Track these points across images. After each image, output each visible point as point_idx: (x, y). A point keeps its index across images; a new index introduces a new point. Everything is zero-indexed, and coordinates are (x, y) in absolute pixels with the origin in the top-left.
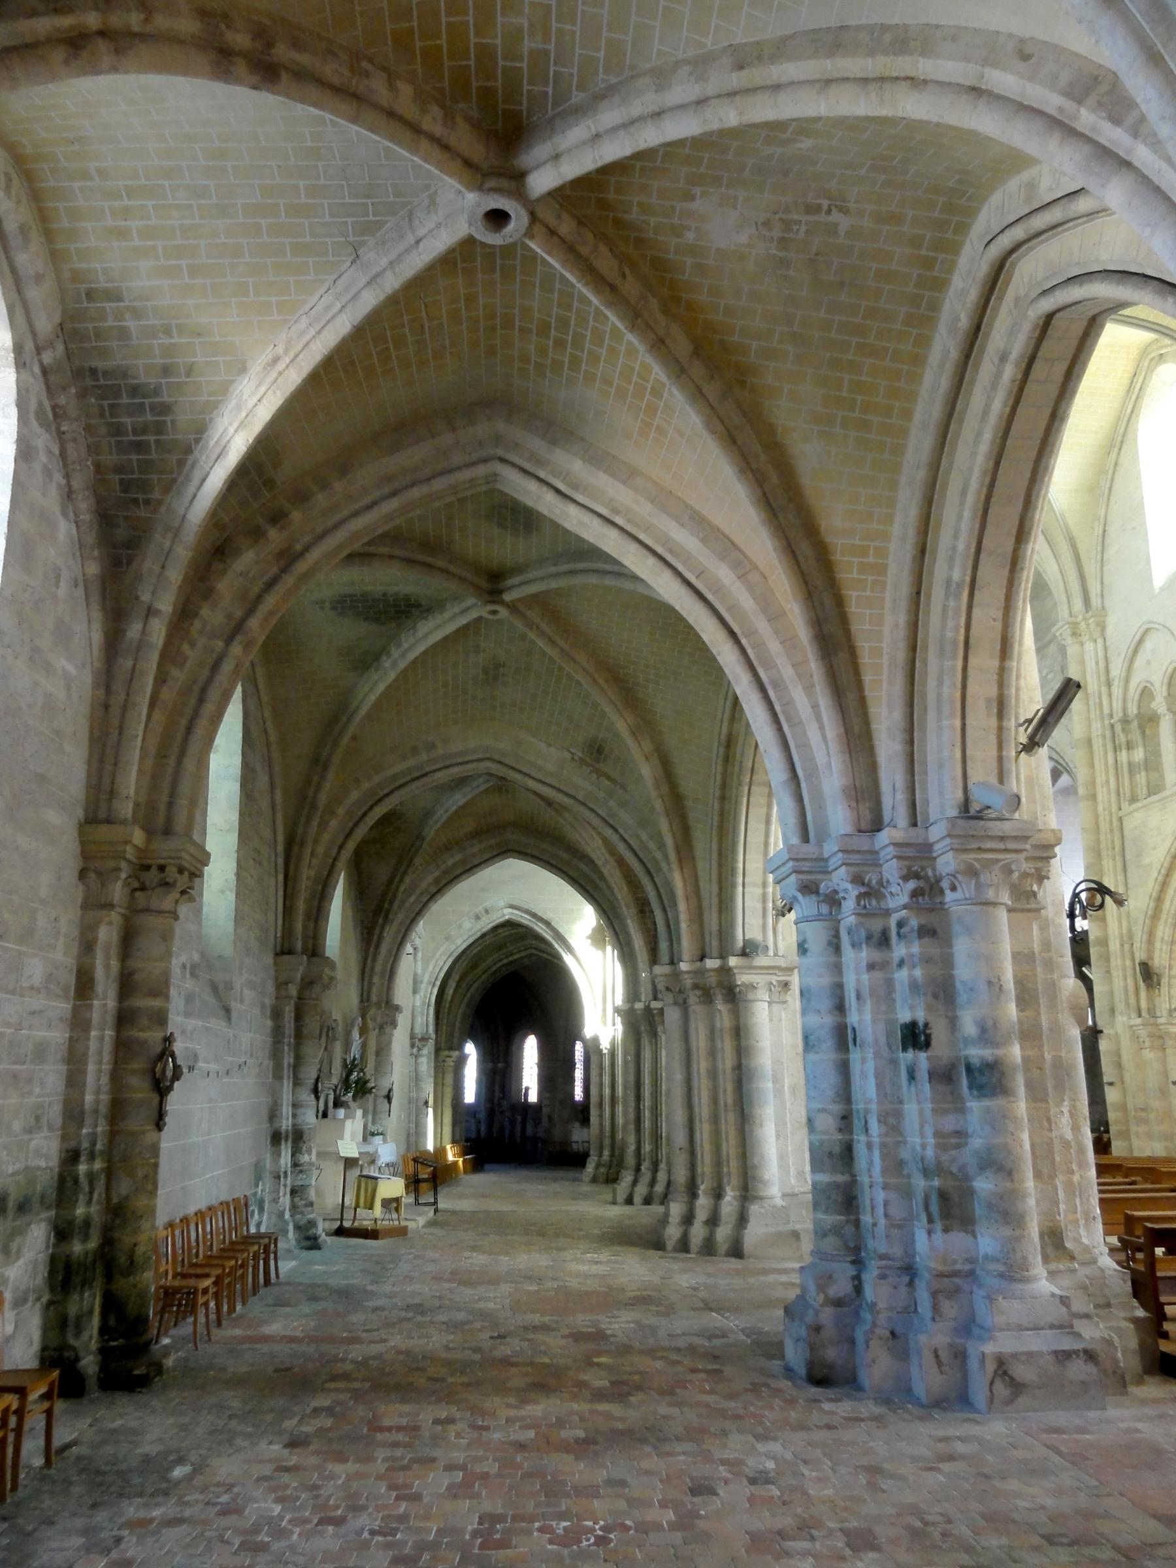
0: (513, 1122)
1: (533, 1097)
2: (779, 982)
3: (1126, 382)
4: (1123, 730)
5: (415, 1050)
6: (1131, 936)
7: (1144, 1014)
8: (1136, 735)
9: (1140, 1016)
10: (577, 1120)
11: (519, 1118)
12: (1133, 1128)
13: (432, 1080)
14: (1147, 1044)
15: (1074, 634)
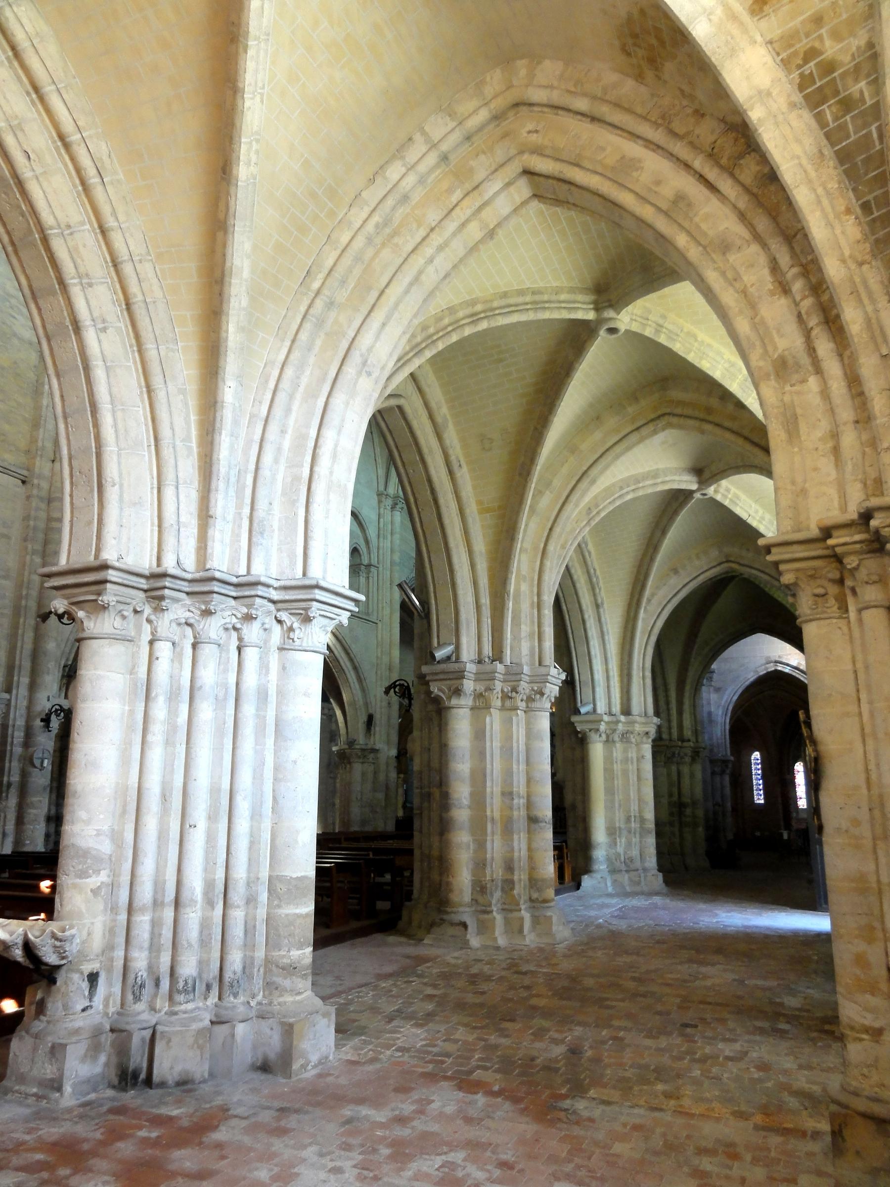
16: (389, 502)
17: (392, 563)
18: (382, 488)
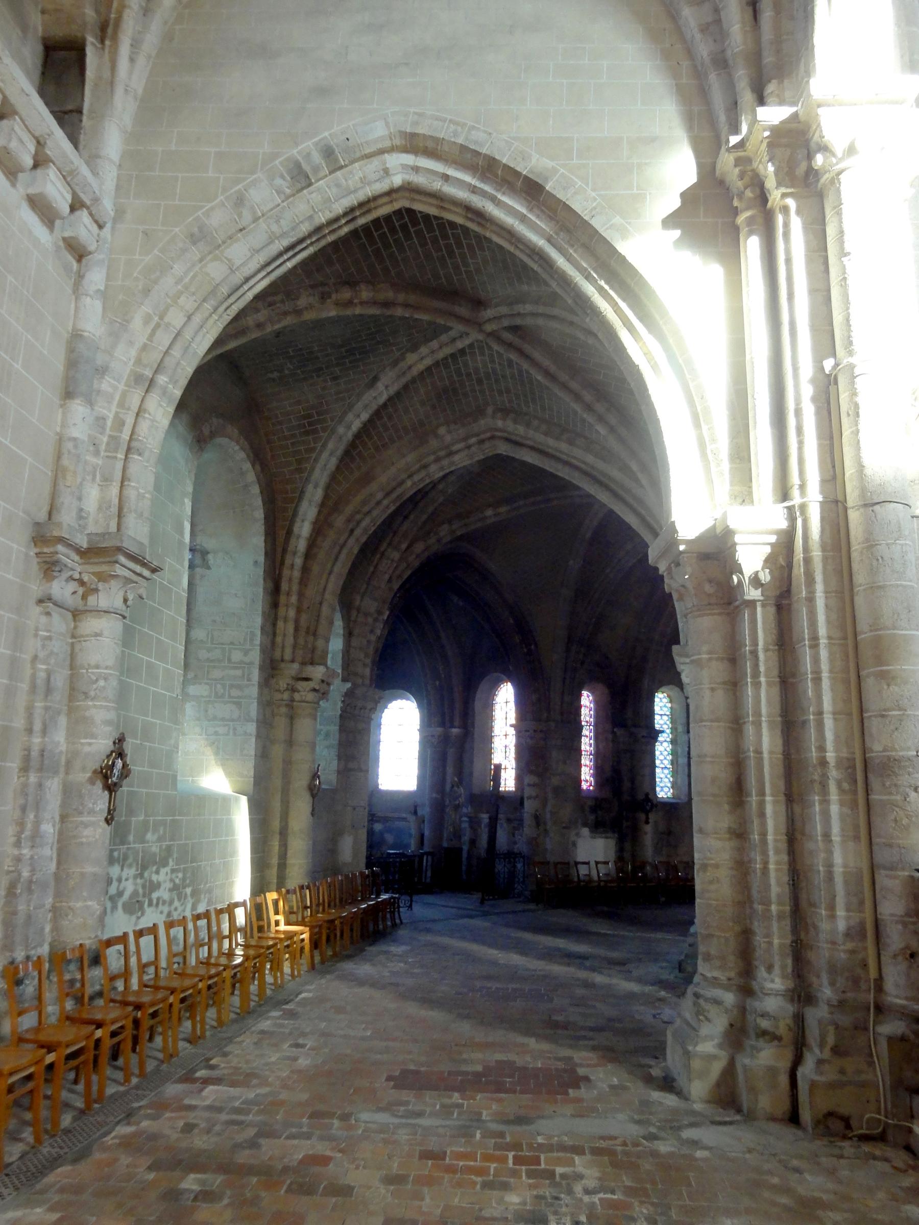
0: (474, 822)
1: (508, 782)
5: (62, 589)
10: (585, 825)
11: (485, 817)
13: (252, 728)
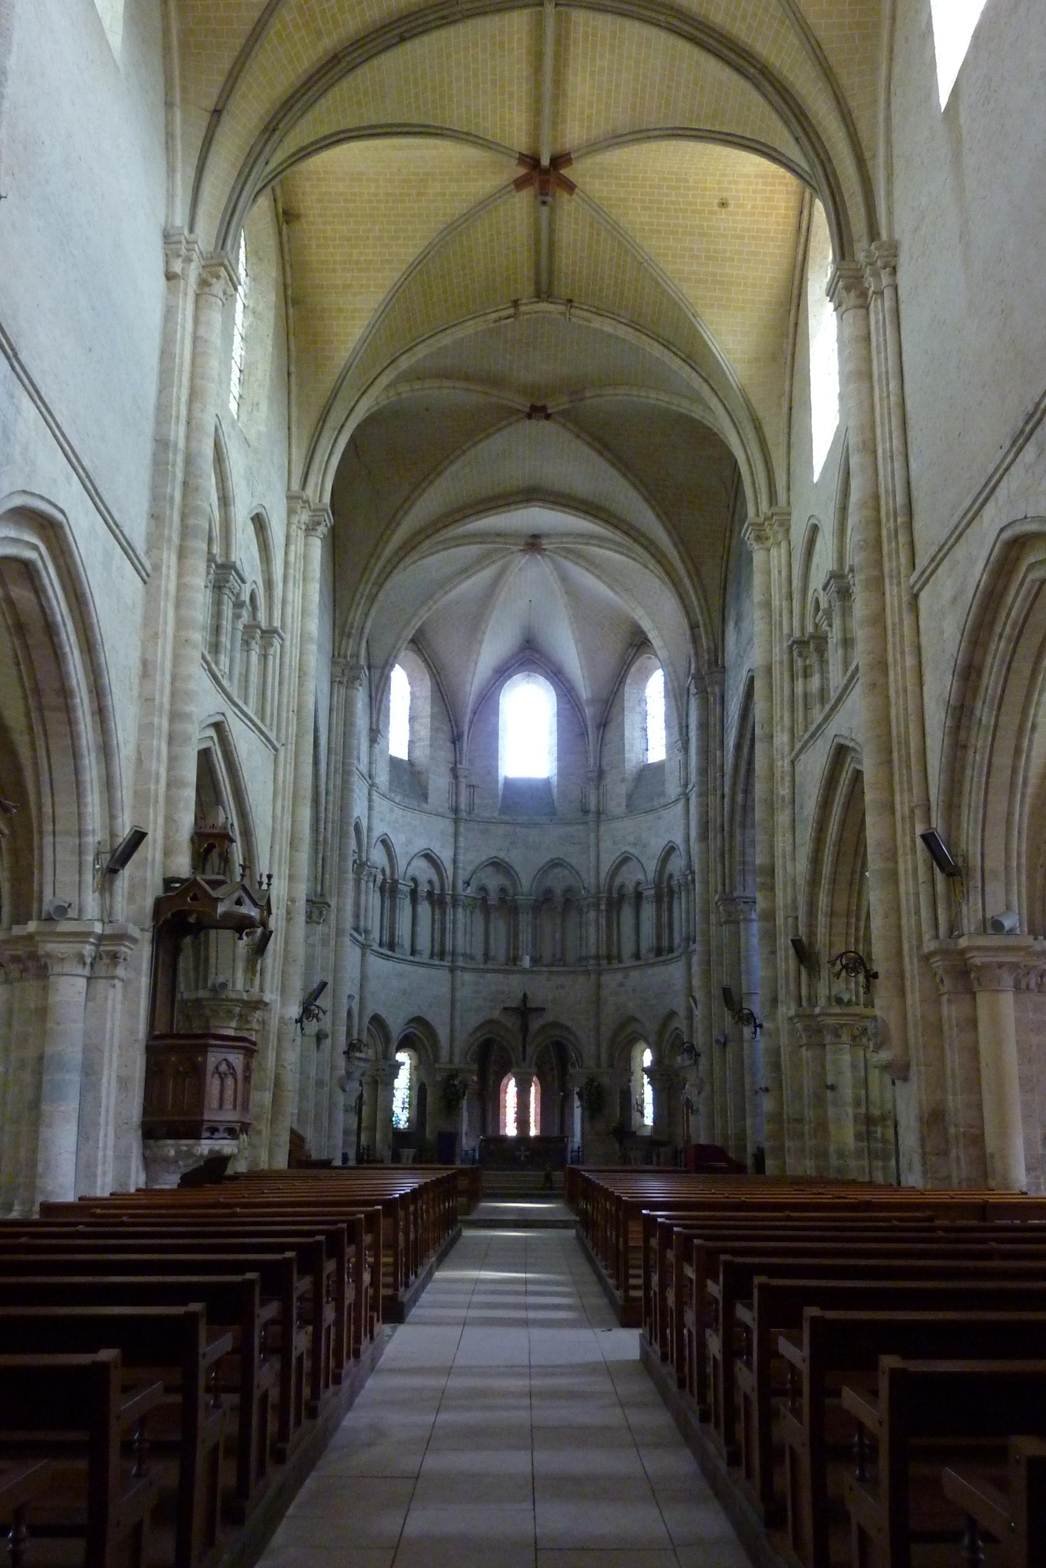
2: (107, 953)
3: (793, 220)
4: (800, 655)
6: (795, 908)
7: (804, 1003)
8: (813, 660)
9: (800, 1005)
12: (787, 1144)
14: (804, 1040)
15: (759, 538)
16: (305, 517)
17: (304, 638)
18: (296, 486)
